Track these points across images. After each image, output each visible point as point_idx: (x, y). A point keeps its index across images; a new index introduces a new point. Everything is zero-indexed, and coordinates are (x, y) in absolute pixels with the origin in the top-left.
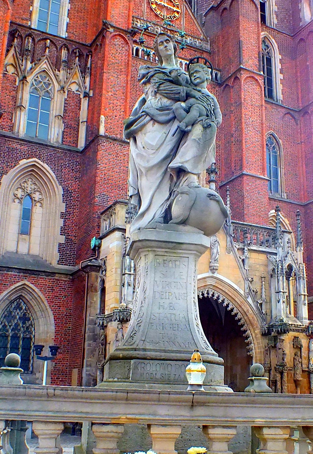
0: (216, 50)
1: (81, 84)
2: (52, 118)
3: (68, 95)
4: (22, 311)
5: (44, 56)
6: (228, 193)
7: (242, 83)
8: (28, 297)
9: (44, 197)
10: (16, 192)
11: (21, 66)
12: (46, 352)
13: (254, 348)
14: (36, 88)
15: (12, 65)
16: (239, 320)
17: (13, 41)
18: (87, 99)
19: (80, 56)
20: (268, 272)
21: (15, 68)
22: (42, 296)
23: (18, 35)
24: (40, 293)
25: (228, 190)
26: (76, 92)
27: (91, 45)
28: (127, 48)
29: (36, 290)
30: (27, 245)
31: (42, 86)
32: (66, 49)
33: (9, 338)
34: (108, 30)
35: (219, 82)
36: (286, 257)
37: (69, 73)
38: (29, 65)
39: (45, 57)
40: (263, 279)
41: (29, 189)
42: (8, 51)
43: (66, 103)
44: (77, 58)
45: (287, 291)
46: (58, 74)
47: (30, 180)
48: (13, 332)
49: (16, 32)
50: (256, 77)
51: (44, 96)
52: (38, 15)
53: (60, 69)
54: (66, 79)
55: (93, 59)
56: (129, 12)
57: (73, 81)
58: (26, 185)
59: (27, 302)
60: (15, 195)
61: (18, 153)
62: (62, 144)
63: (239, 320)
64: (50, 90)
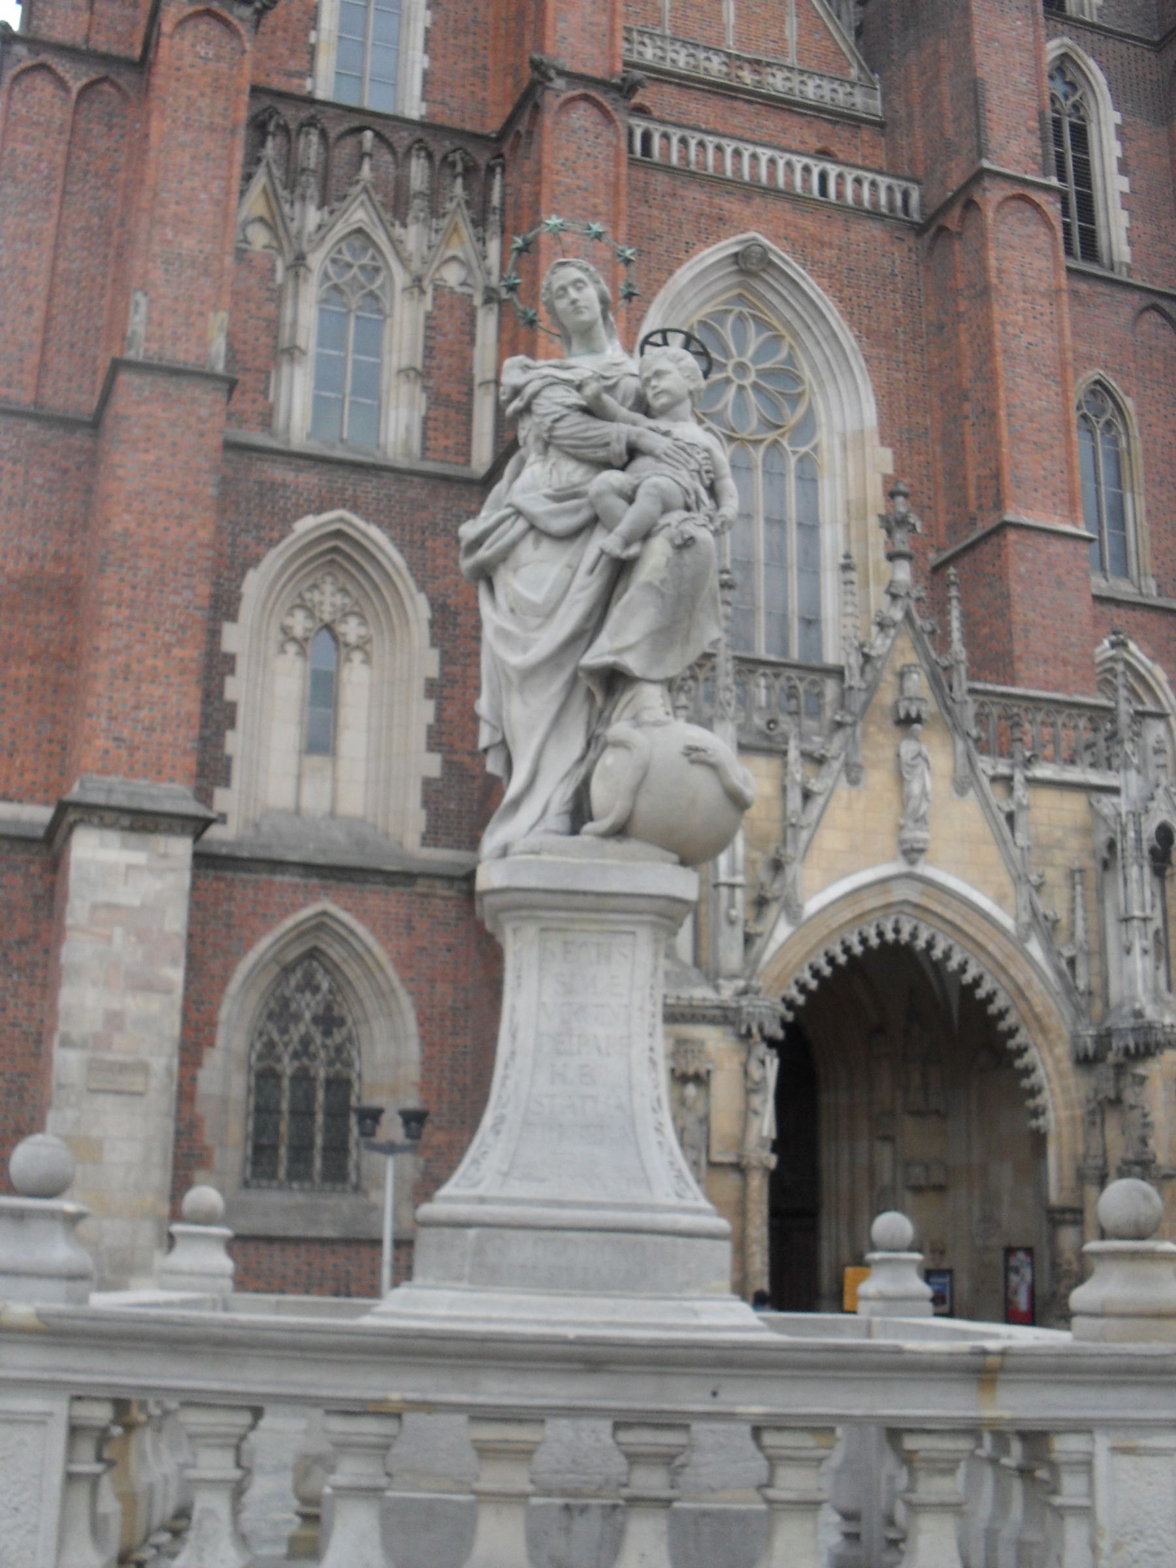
0: (902, 113)
1: (474, 263)
2: (388, 377)
3: (434, 299)
4: (319, 997)
5: (358, 182)
6: (954, 592)
7: (990, 221)
8: (335, 952)
9: (372, 632)
10: (289, 621)
11: (288, 221)
12: (392, 1129)
13: (1050, 1106)
14: (336, 287)
15: (261, 220)
16: (1002, 1015)
17: (263, 143)
18: (495, 307)
19: (469, 171)
20: (1093, 853)
21: (271, 227)
22: (377, 949)
23: (278, 126)
24: (370, 940)
25: (954, 583)
26: (459, 289)
27: (502, 136)
28: (608, 135)
29: (361, 929)
30: (327, 787)
31: (354, 278)
32: (423, 154)
33: (286, 1083)
34: (548, 84)
35: (916, 217)
36: (1152, 798)
37: (437, 231)
38: (313, 216)
39: (359, 187)
40: (1077, 877)
41: (327, 608)
42: (248, 178)
43: (431, 326)
44: (459, 181)
45: (1158, 913)
46: (403, 238)
47: (329, 579)
48: (296, 1064)
49: (271, 117)
50: (1038, 197)
51: (360, 308)
52: (333, 56)
53: (410, 219)
54: (425, 249)
55: (509, 180)
56: (612, 19)
57: (449, 253)
58: (316, 596)
59: (333, 969)
60: (285, 630)
61: (289, 498)
62: (424, 457)
63: (1002, 1015)
64: (382, 287)
